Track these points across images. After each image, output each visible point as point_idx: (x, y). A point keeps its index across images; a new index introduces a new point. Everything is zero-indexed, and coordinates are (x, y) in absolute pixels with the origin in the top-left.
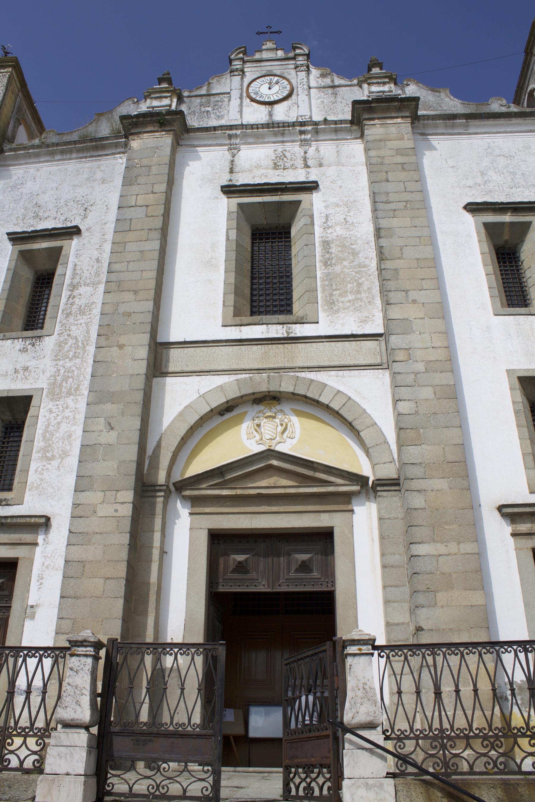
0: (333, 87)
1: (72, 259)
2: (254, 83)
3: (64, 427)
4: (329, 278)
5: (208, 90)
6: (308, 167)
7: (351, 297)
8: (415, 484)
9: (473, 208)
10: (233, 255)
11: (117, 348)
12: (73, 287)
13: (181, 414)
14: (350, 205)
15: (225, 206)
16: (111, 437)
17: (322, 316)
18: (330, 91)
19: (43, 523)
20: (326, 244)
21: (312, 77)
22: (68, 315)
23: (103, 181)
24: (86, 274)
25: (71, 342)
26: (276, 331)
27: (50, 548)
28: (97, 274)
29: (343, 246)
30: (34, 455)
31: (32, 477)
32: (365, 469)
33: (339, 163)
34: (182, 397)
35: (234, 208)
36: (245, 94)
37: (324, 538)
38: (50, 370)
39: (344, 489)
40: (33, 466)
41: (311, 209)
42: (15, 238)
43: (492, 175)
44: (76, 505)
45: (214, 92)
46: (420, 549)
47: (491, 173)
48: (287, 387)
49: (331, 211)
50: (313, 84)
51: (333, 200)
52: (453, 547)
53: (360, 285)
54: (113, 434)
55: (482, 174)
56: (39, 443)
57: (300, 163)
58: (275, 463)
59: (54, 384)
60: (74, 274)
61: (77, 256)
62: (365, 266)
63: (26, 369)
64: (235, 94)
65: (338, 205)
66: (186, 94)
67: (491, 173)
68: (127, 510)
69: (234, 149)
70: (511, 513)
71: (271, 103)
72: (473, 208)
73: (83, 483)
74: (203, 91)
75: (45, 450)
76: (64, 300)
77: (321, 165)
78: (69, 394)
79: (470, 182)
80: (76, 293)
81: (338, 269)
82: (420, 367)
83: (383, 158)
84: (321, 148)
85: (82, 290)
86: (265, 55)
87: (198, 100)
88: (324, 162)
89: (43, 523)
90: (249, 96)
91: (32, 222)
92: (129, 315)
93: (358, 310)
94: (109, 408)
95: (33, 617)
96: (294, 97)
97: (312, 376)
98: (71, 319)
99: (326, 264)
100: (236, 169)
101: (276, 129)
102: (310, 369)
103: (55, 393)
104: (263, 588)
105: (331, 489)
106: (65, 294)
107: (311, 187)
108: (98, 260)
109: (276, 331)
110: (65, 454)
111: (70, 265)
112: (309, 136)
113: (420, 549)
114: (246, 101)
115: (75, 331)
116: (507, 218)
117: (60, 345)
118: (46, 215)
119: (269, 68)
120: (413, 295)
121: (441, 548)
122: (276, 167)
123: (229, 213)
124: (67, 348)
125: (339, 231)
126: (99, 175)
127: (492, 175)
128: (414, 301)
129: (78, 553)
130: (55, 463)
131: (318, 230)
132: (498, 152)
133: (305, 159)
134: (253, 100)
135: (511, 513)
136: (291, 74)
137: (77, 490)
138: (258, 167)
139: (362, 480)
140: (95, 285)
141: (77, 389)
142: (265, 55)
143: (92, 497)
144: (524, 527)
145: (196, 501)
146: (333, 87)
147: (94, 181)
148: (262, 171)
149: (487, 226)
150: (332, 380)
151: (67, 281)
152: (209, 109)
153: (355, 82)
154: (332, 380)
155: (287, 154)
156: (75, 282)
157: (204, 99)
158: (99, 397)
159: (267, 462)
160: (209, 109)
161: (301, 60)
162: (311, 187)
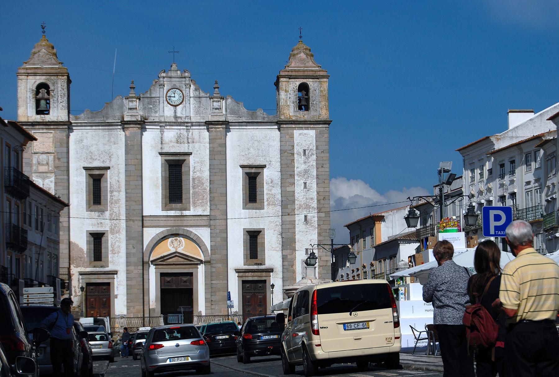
0: (200, 98)
1: (109, 180)
2: (169, 93)
3: (117, 244)
4: (194, 193)
5: (150, 95)
6: (189, 143)
7: (200, 201)
8: (213, 265)
9: (242, 167)
10: (164, 182)
11: (132, 222)
12: (112, 192)
13: (151, 240)
14: (202, 162)
15: (159, 161)
16: (133, 251)
17: (191, 208)
18: (198, 100)
19: (115, 273)
20: (194, 179)
21: (191, 91)
22: (112, 203)
23: (114, 144)
24: (115, 187)
25: (114, 214)
26: (178, 213)
27: (119, 279)
28: (119, 188)
29: (199, 181)
30: (109, 252)
31: (110, 259)
32: (202, 258)
33: (200, 142)
34: (150, 234)
35: (164, 162)
36: (165, 99)
37: (191, 274)
38: (109, 224)
39: (196, 262)
40: (110, 256)
41: (189, 164)
42: (86, 169)
43: (252, 150)
44: (127, 270)
45: (153, 96)
46: (214, 282)
47: (251, 149)
48: (181, 232)
49: (196, 165)
50: (192, 95)
51: (197, 160)
52: (221, 282)
53: (204, 196)
54: (135, 250)
55: (248, 149)
56: (110, 249)
57: (186, 140)
58: (178, 255)
59: (111, 229)
60: (111, 187)
61: (111, 179)
62: (206, 189)
63: (101, 223)
64: (161, 99)
65: (198, 162)
66: (142, 96)
67: (251, 149)
68: (141, 271)
69: (162, 133)
70: (238, 271)
71: (176, 106)
72: (242, 167)
73: (128, 264)
74: (148, 95)
75: (113, 251)
76: (109, 197)
77: (193, 142)
78: (117, 233)
79: (243, 154)
80: (113, 194)
81: (197, 190)
82: (218, 231)
83: (214, 148)
84: (194, 133)
85: (115, 193)
86: (173, 74)
87: (146, 100)
88: (195, 141)
89: (115, 273)
90: (167, 100)
91: (90, 160)
92: (134, 210)
93: (202, 206)
94: (132, 241)
95: (117, 298)
96: (184, 102)
97: (188, 229)
98: (113, 205)
99: (193, 188)
100: (163, 142)
101: (177, 123)
102: (187, 226)
103: (112, 233)
104: (174, 287)
105: (193, 262)
106: (109, 195)
107: (190, 154)
108: (118, 182)
109: (178, 213)
110: (119, 252)
111: (109, 182)
112: (189, 128)
113: (214, 282)
114: (166, 103)
115: (116, 210)
116: (253, 170)
117: (111, 215)
118: (95, 158)
119: (174, 83)
120: (218, 207)
121: (218, 282)
122: (177, 142)
123: (162, 164)
124: (113, 216)
125: (198, 174)
126: (112, 140)
127: (252, 150)
128: (218, 209)
129: (129, 283)
130: (116, 255)
131: (191, 173)
132: (255, 139)
133: (188, 138)
134: (168, 103)
135: (238, 271)
136: (184, 89)
137: (127, 266)
138: (171, 141)
139: (201, 262)
140: (119, 191)
141: (119, 231)
142: (173, 74)
143: (132, 268)
144: (241, 274)
145: (155, 265)
146: (200, 98)
147: (111, 142)
148: (173, 144)
149: (247, 174)
150: (194, 230)
151: (109, 190)
152: (151, 106)
153: (208, 95)
154: (194, 230)
155: (182, 135)
156: (112, 189)
157: (149, 99)
158: (129, 238)
159: (176, 254)
160: (151, 106)
161: (187, 81)
162: (190, 154)
